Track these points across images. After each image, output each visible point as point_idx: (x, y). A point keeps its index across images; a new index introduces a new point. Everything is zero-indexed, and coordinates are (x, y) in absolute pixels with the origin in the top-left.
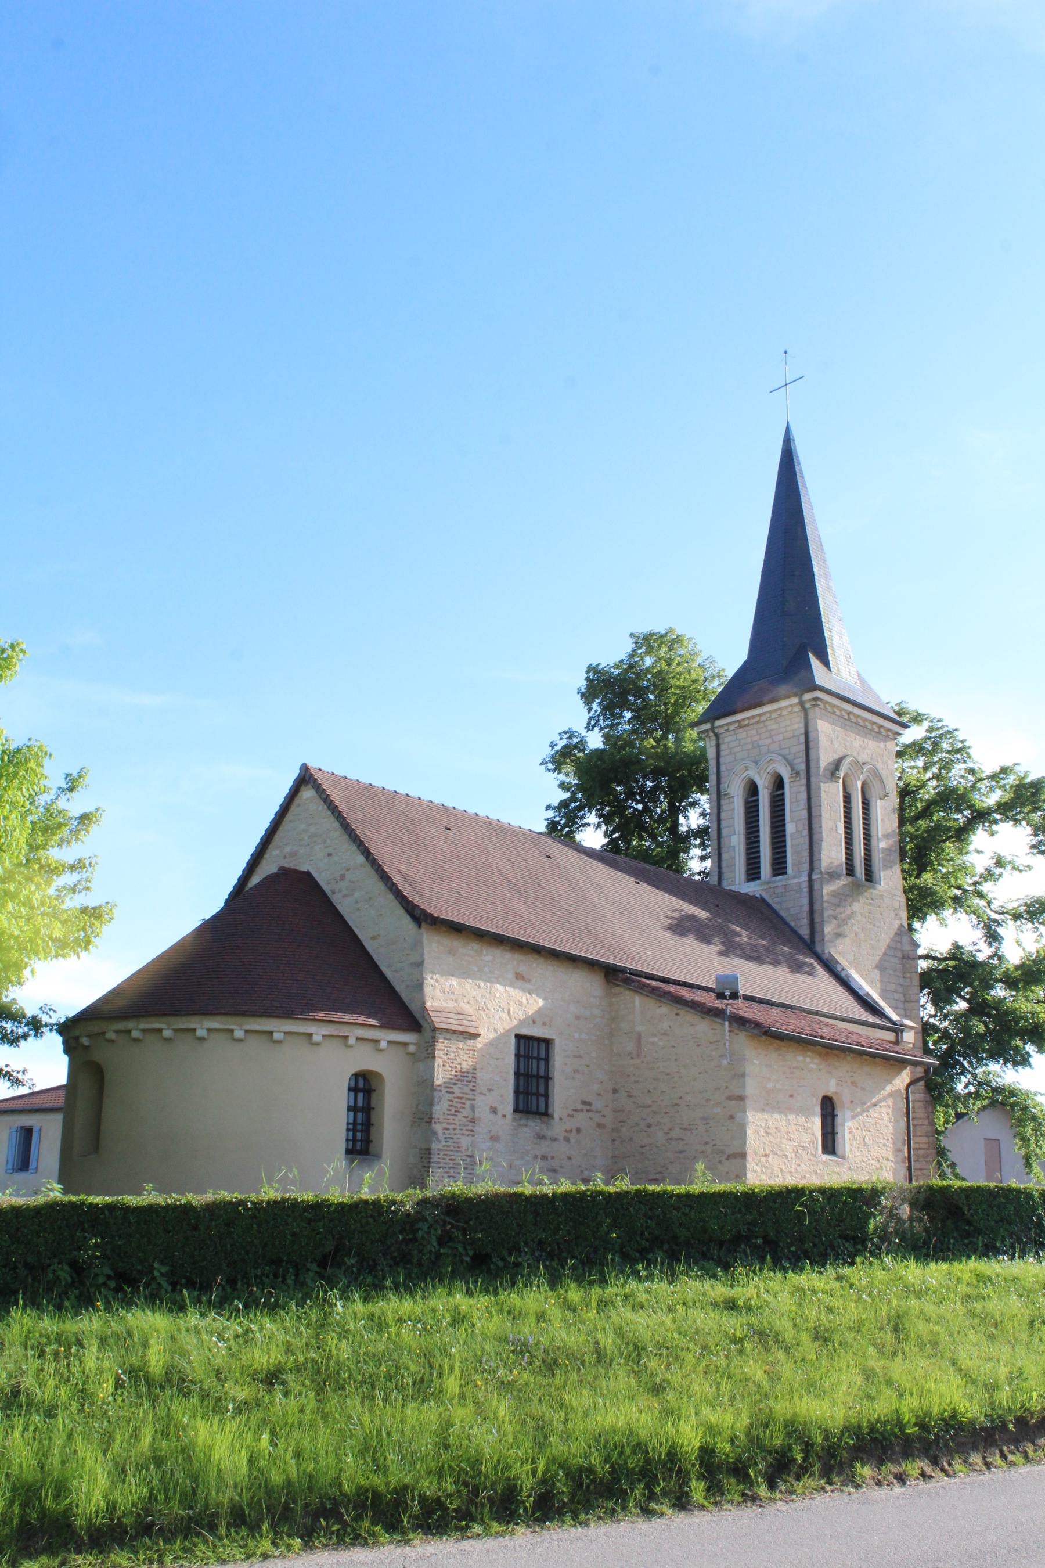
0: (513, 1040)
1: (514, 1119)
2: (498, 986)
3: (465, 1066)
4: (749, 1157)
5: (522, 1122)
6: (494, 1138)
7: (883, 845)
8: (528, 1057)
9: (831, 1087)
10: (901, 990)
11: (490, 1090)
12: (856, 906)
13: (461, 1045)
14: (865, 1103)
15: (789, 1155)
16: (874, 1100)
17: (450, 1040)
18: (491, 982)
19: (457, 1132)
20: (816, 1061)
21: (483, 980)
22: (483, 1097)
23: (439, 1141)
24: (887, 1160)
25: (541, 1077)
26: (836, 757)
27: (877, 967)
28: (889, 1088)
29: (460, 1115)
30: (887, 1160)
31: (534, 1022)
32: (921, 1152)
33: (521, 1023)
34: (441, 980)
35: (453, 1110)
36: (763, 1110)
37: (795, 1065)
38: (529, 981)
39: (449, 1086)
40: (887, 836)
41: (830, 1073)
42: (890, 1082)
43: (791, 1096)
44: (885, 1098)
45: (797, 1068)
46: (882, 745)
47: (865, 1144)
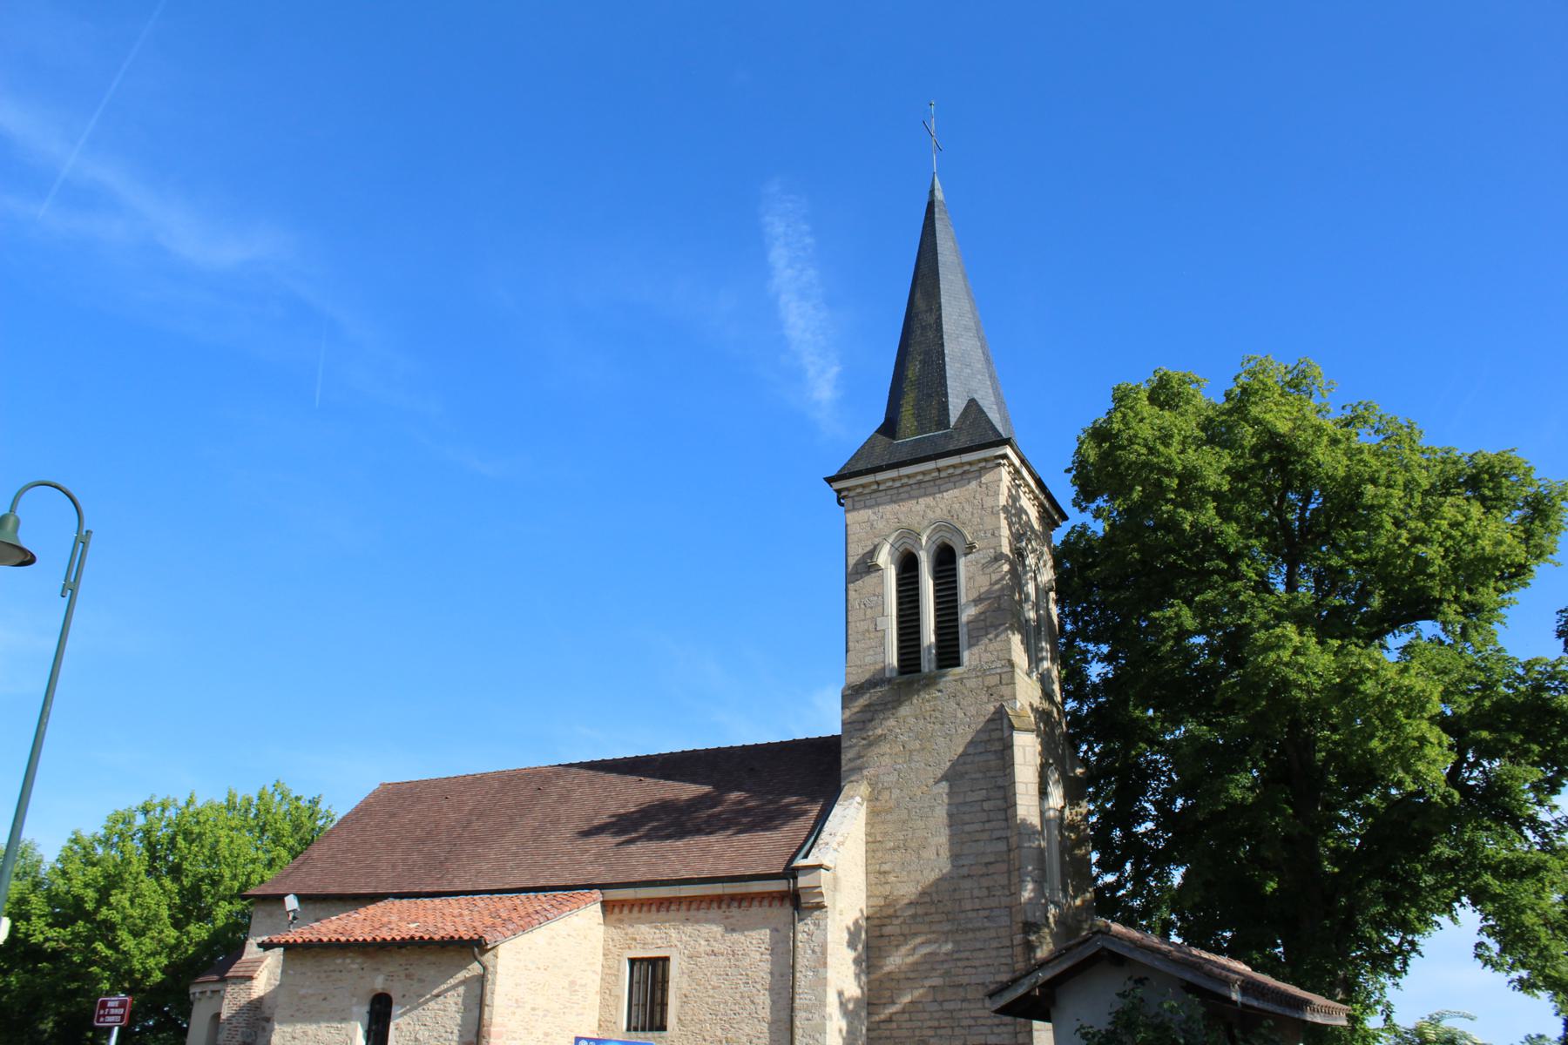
9: (379, 984)
10: (1000, 794)
12: (904, 710)
16: (435, 992)
20: (359, 960)
26: (876, 541)
27: (945, 778)
28: (461, 976)
39: (229, 1019)
42: (463, 967)
44: (454, 987)
46: (974, 484)
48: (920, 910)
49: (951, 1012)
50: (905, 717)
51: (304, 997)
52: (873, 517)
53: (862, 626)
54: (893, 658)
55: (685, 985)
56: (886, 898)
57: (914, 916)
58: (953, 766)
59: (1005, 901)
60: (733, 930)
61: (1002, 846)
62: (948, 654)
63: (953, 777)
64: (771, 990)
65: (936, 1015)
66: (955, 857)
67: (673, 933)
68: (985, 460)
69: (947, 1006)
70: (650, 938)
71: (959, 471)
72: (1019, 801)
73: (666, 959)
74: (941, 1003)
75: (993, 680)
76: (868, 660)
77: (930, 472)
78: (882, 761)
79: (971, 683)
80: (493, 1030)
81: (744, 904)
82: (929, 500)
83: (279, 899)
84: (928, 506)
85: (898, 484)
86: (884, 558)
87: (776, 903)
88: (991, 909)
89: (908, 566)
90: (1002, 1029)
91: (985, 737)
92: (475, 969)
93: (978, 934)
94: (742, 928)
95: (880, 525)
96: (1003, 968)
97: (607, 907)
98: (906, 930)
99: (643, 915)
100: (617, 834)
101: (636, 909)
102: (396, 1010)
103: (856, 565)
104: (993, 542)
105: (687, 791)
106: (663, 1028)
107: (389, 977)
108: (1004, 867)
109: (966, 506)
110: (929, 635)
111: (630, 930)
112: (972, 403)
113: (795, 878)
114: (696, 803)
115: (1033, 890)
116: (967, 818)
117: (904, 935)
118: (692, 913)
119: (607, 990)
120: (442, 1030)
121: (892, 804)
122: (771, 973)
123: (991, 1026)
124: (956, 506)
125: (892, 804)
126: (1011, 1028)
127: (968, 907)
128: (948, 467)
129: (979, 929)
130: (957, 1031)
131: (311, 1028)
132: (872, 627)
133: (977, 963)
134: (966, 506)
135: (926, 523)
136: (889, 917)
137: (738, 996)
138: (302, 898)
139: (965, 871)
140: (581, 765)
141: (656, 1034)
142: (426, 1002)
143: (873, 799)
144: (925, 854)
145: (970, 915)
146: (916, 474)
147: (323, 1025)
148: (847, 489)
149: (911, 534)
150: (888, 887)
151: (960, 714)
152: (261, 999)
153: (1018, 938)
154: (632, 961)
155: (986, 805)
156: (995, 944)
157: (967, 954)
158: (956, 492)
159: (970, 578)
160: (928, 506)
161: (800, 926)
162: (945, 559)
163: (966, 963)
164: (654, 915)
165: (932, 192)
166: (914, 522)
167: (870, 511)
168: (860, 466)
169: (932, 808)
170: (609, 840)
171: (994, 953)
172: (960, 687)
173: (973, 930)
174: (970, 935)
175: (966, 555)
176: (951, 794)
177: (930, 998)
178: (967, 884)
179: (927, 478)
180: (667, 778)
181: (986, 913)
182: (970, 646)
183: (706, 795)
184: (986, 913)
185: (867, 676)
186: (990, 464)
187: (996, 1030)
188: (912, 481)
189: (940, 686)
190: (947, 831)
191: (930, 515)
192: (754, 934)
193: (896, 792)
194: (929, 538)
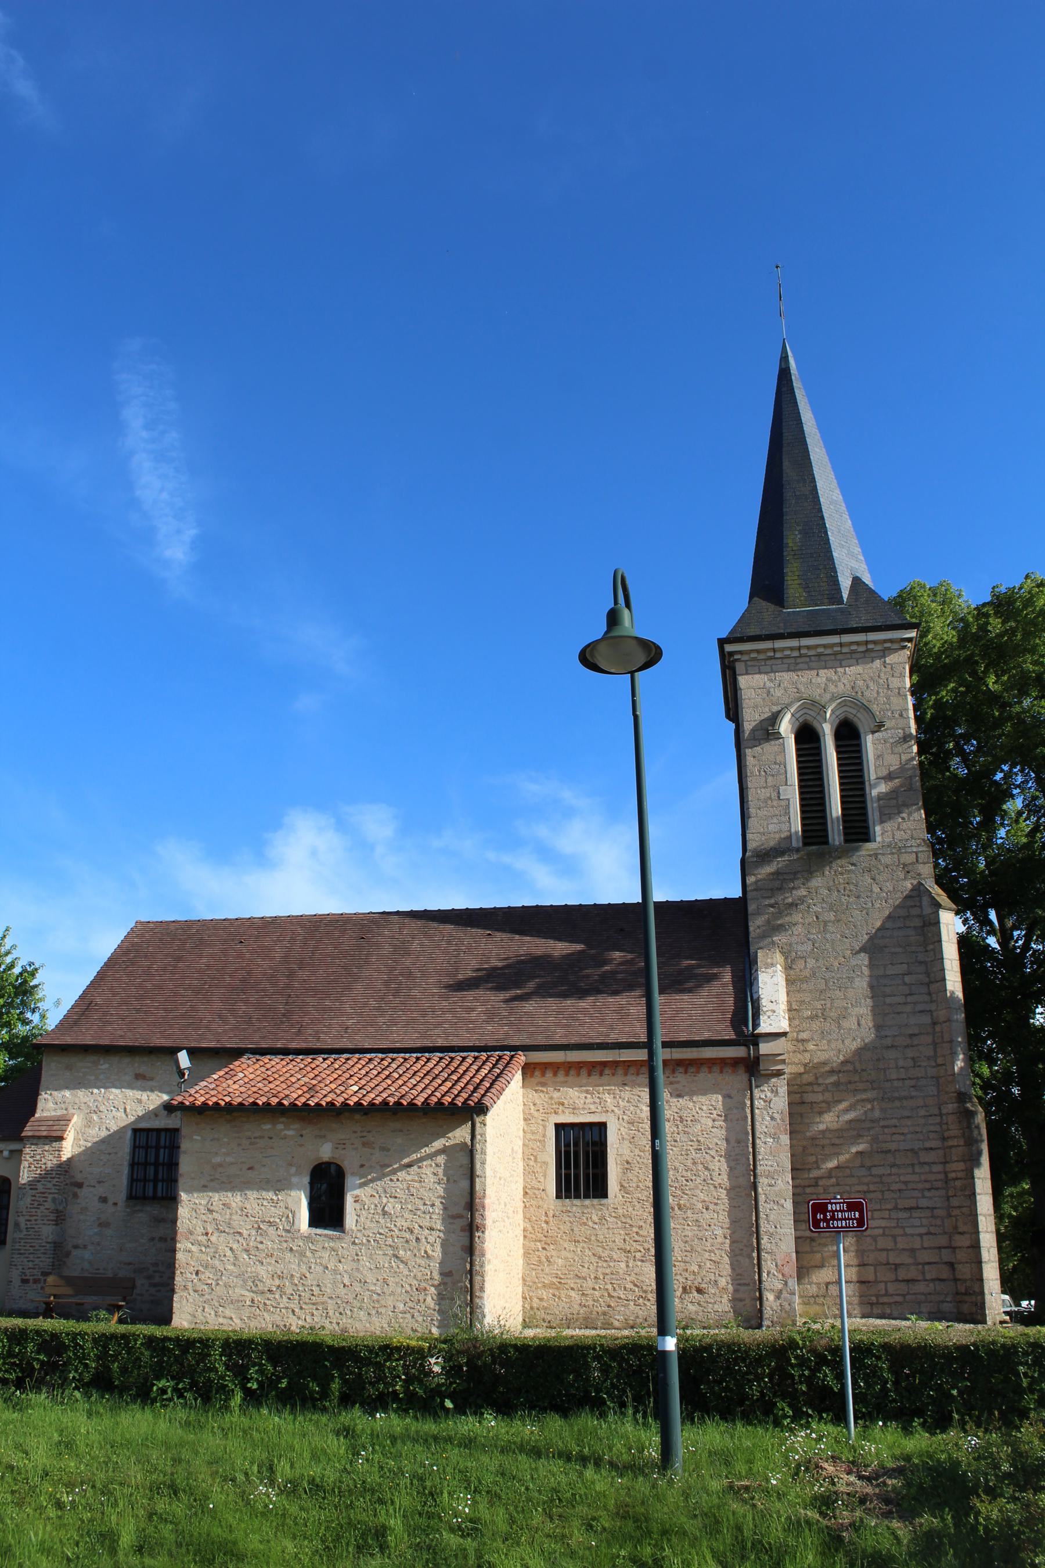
0: (129, 1133)
1: (127, 1206)
2: (113, 1090)
3: (49, 1165)
4: (179, 1237)
5: (137, 1208)
6: (103, 1225)
7: (882, 788)
8: (147, 1148)
9: (326, 1152)
11: (99, 1182)
12: (816, 882)
13: (47, 1148)
14: (389, 1166)
15: (245, 1233)
16: (406, 1161)
17: (36, 1144)
18: (106, 1088)
19: (39, 1222)
20: (297, 1126)
21: (98, 1088)
22: (91, 1189)
23: (21, 1231)
24: (432, 1229)
25: (150, 1164)
26: (775, 709)
27: (863, 949)
28: (438, 1144)
29: (42, 1208)
30: (432, 1229)
31: (156, 1116)
32: (958, 1183)
33: (140, 1119)
34: (55, 1093)
35: (36, 1203)
36: (205, 1186)
37: (257, 1134)
38: (152, 1079)
39: (32, 1184)
40: (889, 777)
41: (321, 1137)
43: (249, 1169)
45: (261, 1137)
46: (878, 663)
47: (385, 1213)
48: (843, 1078)
49: (881, 1176)
50: (817, 888)
51: (220, 1165)
52: (769, 684)
53: (764, 793)
54: (797, 825)
55: (626, 1152)
56: (805, 1065)
57: (837, 1084)
58: (871, 939)
59: (931, 1072)
60: (679, 1096)
61: (926, 1019)
62: (857, 830)
63: (873, 948)
64: (728, 1156)
65: (865, 1180)
66: (878, 1027)
67: (609, 1099)
68: (891, 641)
69: (875, 1171)
70: (580, 1103)
71: (862, 648)
72: (947, 977)
73: (602, 1126)
74: (869, 1168)
75: (910, 858)
76: (771, 827)
77: (832, 645)
78: (799, 927)
79: (887, 859)
80: (487, 1201)
81: (691, 1070)
82: (830, 673)
83: (173, 1051)
84: (829, 680)
85: (796, 654)
86: (786, 727)
87: (729, 1070)
88: (918, 1078)
89: (807, 737)
90: (933, 1193)
91: (903, 912)
92: (461, 1134)
93: (905, 1103)
94: (691, 1094)
95: (778, 693)
96: (932, 1135)
97: (528, 1070)
98: (828, 1096)
99: (570, 1079)
100: (499, 988)
101: (561, 1073)
102: (350, 1181)
103: (753, 730)
104: (901, 723)
105: (559, 948)
106: (605, 1195)
107: (340, 1145)
108: (929, 1039)
109: (871, 684)
110: (835, 807)
111: (556, 1095)
112: (857, 581)
113: (756, 1045)
114: (571, 962)
115: (963, 1060)
116: (888, 990)
117: (828, 1103)
118: (630, 1078)
119: (530, 1157)
120: (419, 1203)
121: (807, 973)
122: (727, 1140)
123: (922, 1190)
124: (860, 683)
125: (807, 973)
126: (942, 1192)
127: (894, 1076)
128: (852, 643)
129: (906, 1098)
130: (887, 1195)
131: (235, 1199)
132: (774, 795)
133: (906, 1131)
134: (871, 684)
135: (828, 696)
136: (810, 1084)
137: (689, 1163)
138: (192, 1052)
139: (888, 1042)
140: (413, 915)
141: (596, 1201)
142: (394, 1172)
143: (788, 968)
144: (845, 1024)
145: (896, 1084)
146: (817, 646)
147: (252, 1195)
148: (740, 653)
149: (817, 706)
150: (807, 1056)
151: (876, 889)
152: (69, 1160)
153: (951, 1107)
154: (558, 1126)
155: (907, 979)
156: (922, 1112)
157: (894, 1122)
158: (859, 669)
159: (879, 757)
160: (829, 680)
161: (757, 1093)
162: (848, 736)
163: (894, 1130)
164: (584, 1078)
165: (784, 358)
166: (816, 693)
167: (765, 677)
168: (753, 631)
169: (851, 979)
170: (495, 998)
171: (923, 1121)
172: (874, 862)
173: (900, 1099)
174: (897, 1103)
175: (873, 732)
176: (871, 966)
177: (858, 1163)
178: (892, 1054)
179: (828, 651)
180: (522, 933)
181: (912, 1082)
182: (882, 822)
183: (580, 952)
184: (912, 1082)
185: (772, 844)
186: (896, 646)
187: (927, 1194)
188: (812, 653)
189: (854, 859)
190: (869, 1002)
191: (832, 688)
192: (703, 1099)
193: (811, 963)
194: (833, 712)
